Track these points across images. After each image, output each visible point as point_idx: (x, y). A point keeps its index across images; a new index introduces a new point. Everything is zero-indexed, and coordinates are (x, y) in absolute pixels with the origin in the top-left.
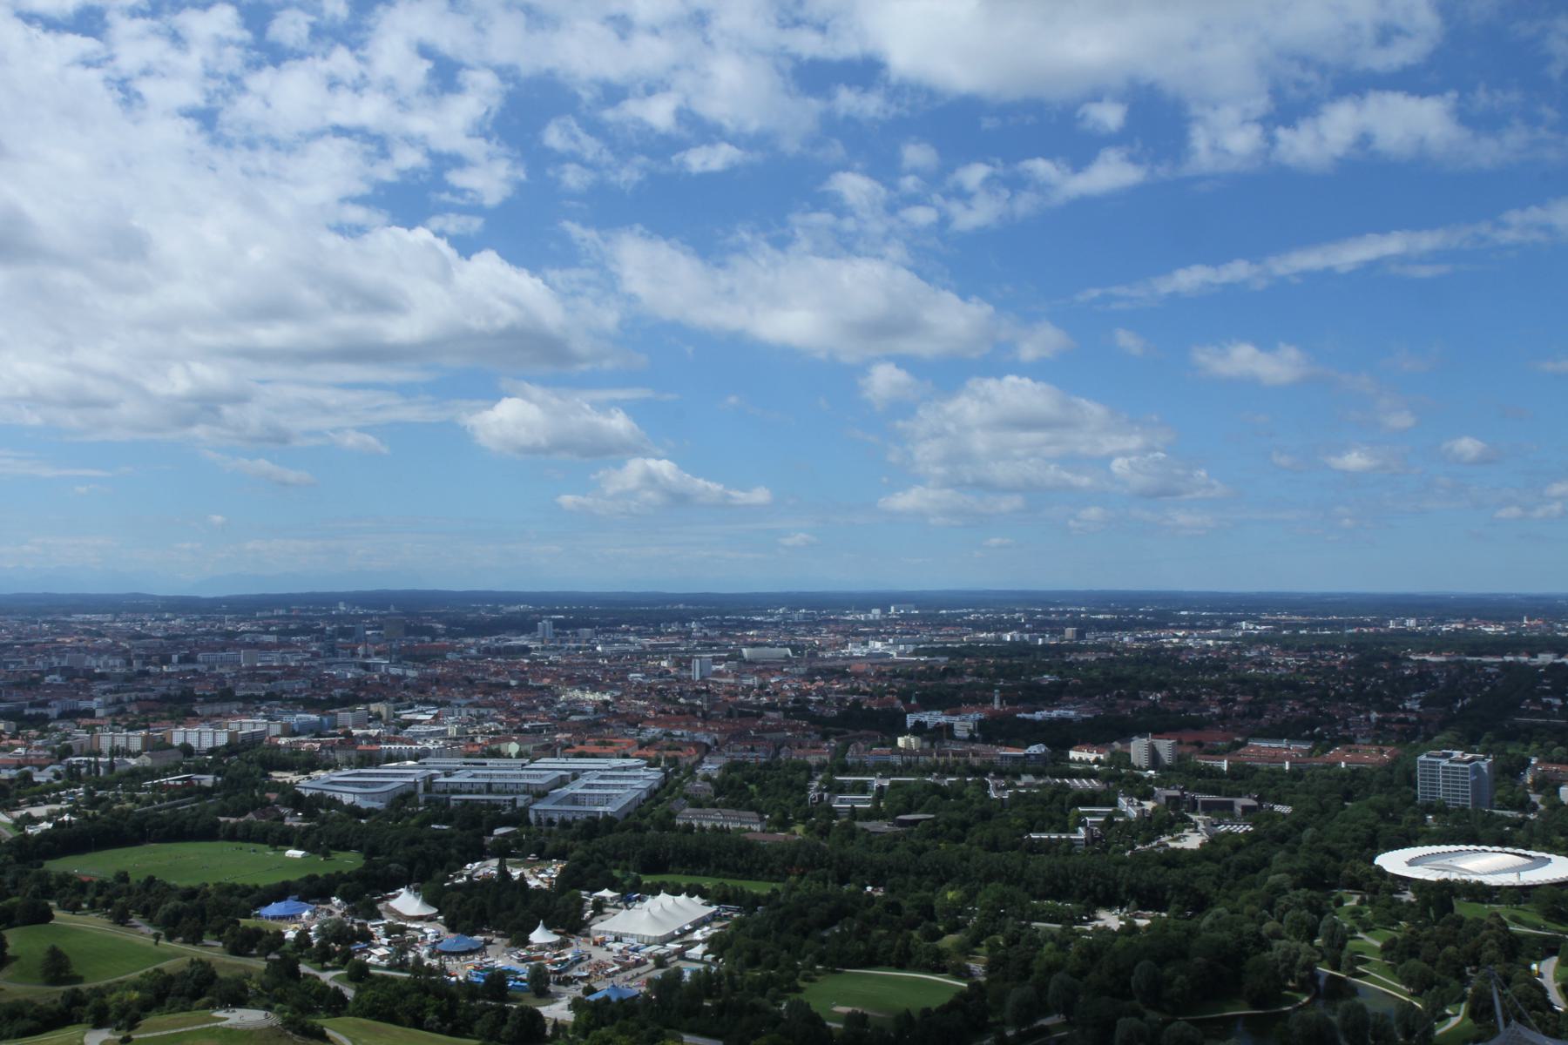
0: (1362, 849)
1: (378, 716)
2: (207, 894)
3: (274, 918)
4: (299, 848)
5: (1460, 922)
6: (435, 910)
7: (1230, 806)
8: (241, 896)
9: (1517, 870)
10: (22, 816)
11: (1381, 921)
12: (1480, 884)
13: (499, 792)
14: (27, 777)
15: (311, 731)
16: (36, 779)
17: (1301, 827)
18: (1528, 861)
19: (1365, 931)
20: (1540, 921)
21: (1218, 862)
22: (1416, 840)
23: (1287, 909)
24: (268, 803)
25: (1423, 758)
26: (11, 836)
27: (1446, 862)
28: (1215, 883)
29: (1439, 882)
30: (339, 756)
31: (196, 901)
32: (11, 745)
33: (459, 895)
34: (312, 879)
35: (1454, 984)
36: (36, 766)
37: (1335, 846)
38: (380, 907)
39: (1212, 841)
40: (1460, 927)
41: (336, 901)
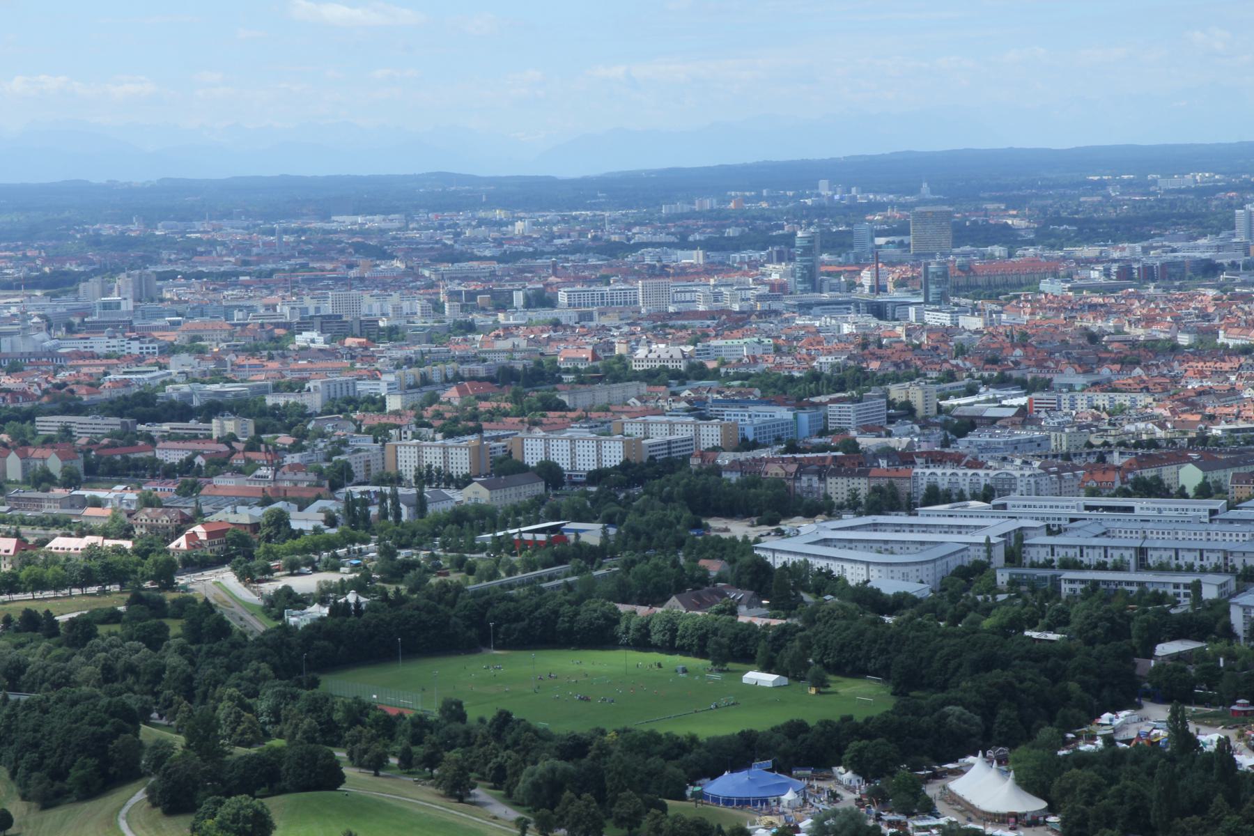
1: (908, 411)
2: (604, 751)
3: (728, 802)
4: (767, 669)
6: (1040, 805)
8: (667, 757)
10: (278, 593)
13: (1162, 568)
14: (280, 520)
15: (778, 440)
16: (295, 525)
24: (703, 580)
26: (262, 629)
30: (838, 488)
31: (586, 761)
32: (249, 461)
33: (1087, 775)
34: (796, 729)
36: (294, 500)
38: (932, 790)
41: (845, 775)
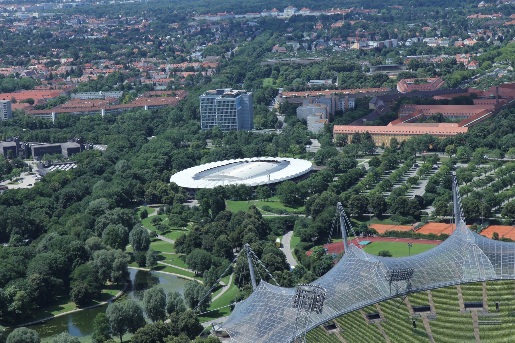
0: (161, 171)
5: (229, 217)
7: (58, 150)
9: (268, 173)
11: (175, 224)
12: (243, 186)
17: (114, 160)
18: (275, 165)
19: (164, 234)
20: (282, 207)
21: (50, 196)
22: (199, 159)
23: (105, 225)
25: (204, 95)
27: (220, 173)
28: (47, 213)
29: (215, 189)
35: (225, 261)
37: (140, 172)
39: (44, 180)
40: (229, 220)
